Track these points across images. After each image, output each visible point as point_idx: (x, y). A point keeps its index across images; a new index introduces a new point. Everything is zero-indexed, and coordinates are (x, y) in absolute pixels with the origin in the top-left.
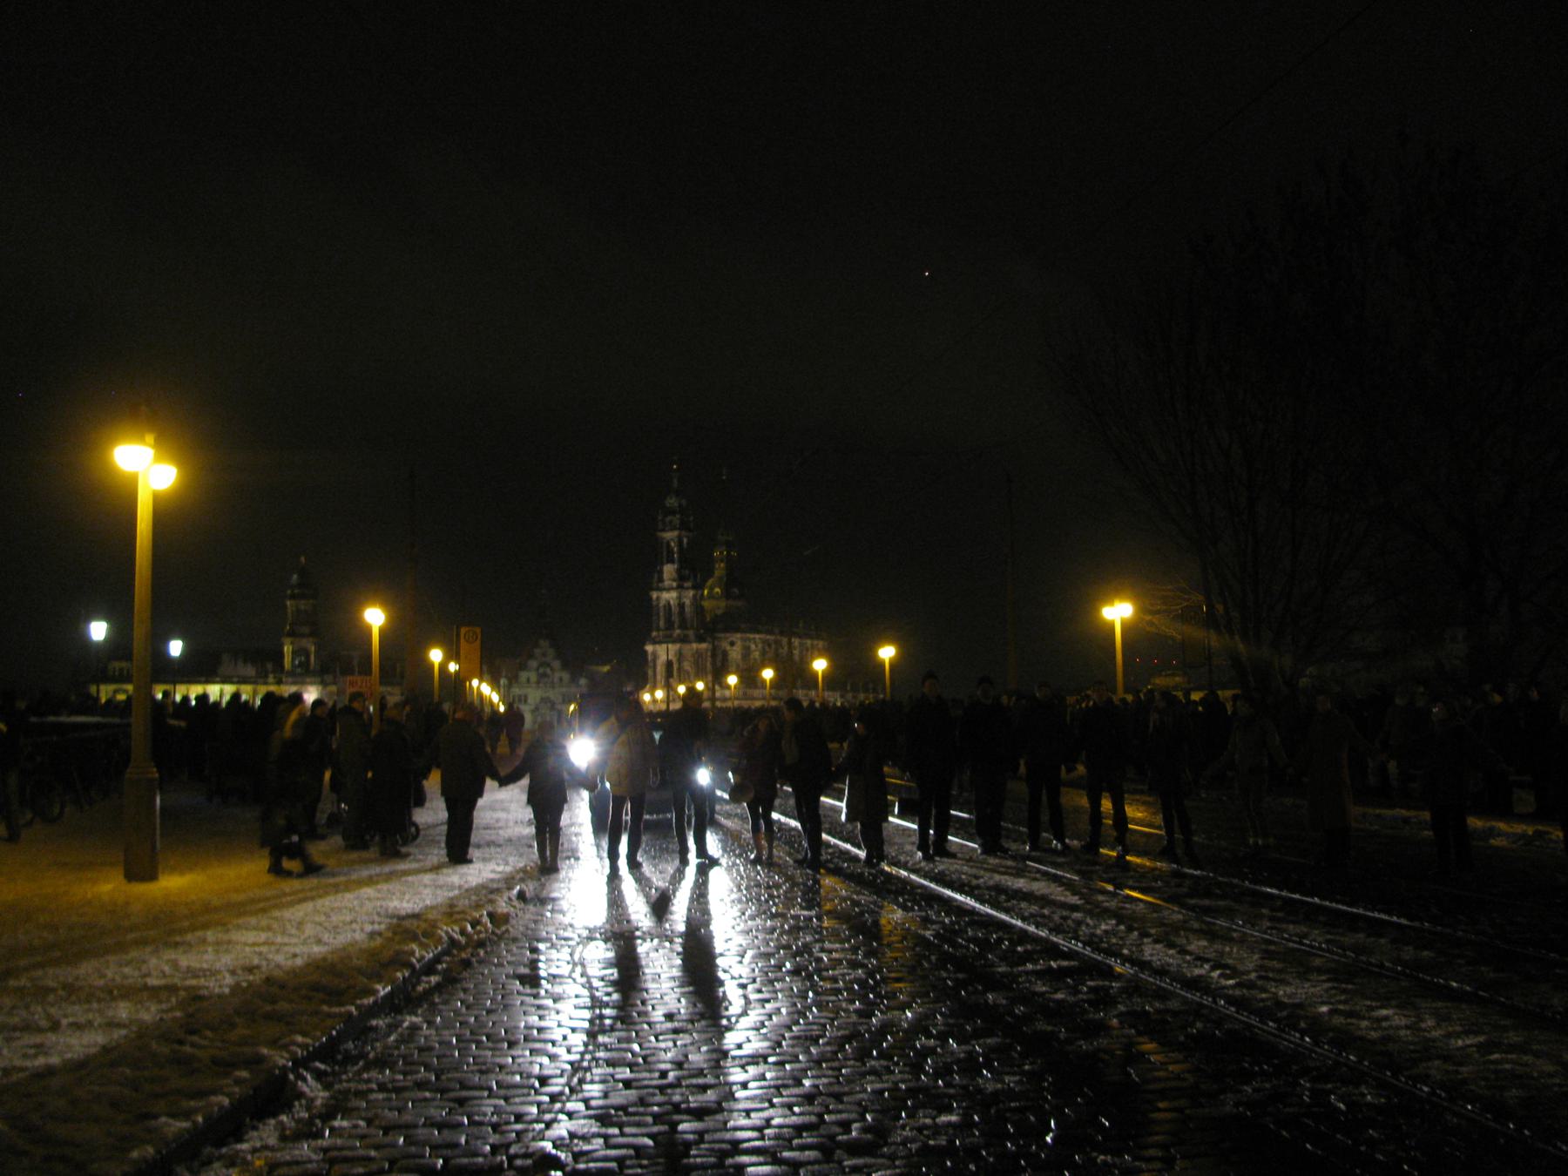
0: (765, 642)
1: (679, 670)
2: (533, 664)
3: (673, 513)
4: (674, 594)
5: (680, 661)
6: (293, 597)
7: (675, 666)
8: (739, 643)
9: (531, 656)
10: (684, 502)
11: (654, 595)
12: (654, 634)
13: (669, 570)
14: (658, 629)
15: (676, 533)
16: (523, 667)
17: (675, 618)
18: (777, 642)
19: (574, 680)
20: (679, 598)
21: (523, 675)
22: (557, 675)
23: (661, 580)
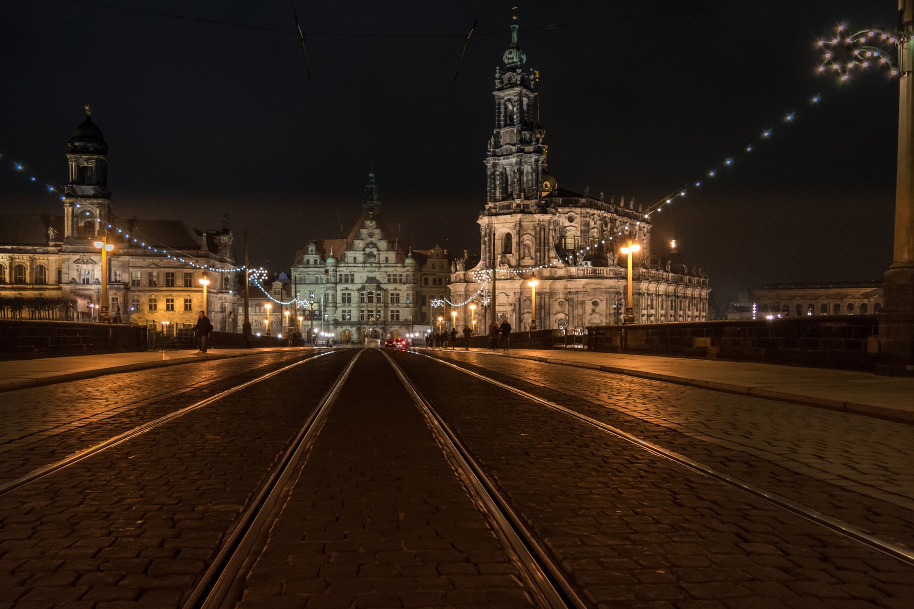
0: (603, 219)
1: (519, 243)
2: (359, 244)
3: (513, 69)
4: (513, 160)
5: (519, 234)
6: (74, 151)
7: (514, 240)
8: (578, 219)
9: (358, 237)
10: (524, 57)
13: (507, 135)
14: (495, 201)
15: (517, 89)
16: (350, 247)
18: (613, 221)
19: (401, 260)
20: (520, 163)
21: (350, 255)
22: (383, 256)
23: (498, 145)
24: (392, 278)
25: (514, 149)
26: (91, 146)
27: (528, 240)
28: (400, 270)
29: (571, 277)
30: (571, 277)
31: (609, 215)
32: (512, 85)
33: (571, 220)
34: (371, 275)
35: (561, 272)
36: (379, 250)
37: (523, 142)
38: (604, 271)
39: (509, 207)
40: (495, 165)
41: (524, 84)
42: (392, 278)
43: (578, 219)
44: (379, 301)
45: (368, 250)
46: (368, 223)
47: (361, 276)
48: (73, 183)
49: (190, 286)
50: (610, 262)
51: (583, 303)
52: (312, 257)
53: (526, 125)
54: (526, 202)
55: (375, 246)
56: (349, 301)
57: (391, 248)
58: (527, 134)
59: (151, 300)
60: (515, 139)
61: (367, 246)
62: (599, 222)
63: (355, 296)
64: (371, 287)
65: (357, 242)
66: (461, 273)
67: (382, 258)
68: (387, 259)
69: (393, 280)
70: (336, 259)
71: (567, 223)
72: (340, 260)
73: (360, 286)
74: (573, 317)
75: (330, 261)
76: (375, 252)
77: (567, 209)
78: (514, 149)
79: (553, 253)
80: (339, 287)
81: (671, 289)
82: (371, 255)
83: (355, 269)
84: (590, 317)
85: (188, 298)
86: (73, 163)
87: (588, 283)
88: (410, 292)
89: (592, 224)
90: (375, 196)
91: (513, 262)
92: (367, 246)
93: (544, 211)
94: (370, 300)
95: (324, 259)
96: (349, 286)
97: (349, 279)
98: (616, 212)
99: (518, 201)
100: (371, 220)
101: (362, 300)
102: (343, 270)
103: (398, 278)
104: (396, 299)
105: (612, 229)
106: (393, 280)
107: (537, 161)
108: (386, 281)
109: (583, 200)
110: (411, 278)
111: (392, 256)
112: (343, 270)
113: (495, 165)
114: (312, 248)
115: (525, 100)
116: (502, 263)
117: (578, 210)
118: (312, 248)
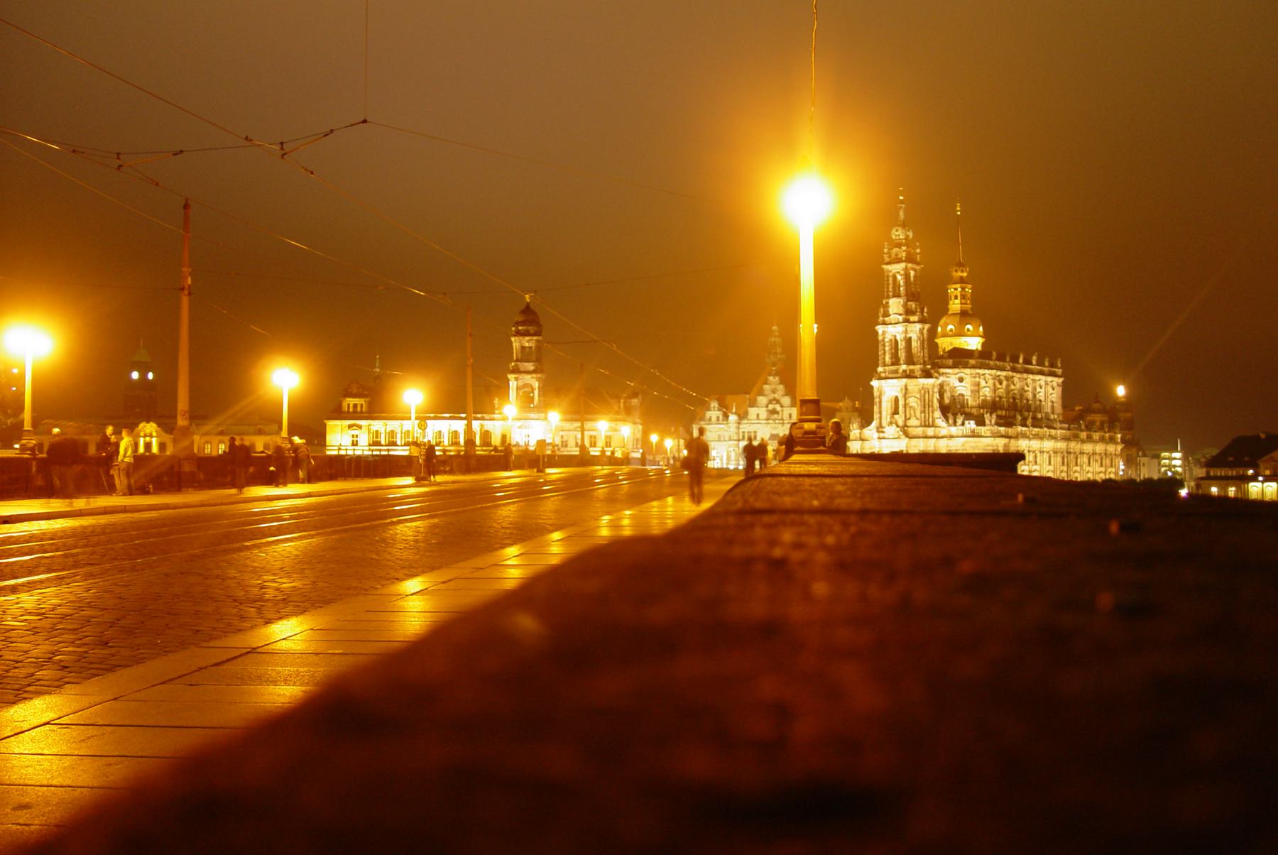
0: (996, 378)
1: (905, 406)
2: (762, 400)
3: (899, 245)
4: (900, 328)
5: (905, 396)
6: (518, 333)
7: (901, 403)
8: (968, 380)
9: (761, 393)
10: (911, 234)
11: (880, 329)
12: (880, 369)
13: (895, 305)
14: (885, 365)
15: (903, 265)
16: (753, 404)
17: (902, 355)
21: (753, 411)
22: (786, 412)
23: (887, 314)
25: (901, 318)
26: (532, 329)
27: (913, 402)
29: (951, 437)
30: (951, 437)
31: (1004, 373)
32: (899, 261)
33: (961, 380)
34: (775, 432)
35: (943, 432)
37: (908, 312)
38: (982, 430)
39: (896, 372)
40: (884, 333)
41: (910, 259)
43: (968, 380)
45: (771, 407)
46: (771, 378)
48: (517, 360)
50: (987, 422)
52: (714, 413)
53: (911, 296)
54: (912, 367)
55: (778, 402)
58: (912, 305)
60: (901, 310)
61: (770, 402)
62: (991, 382)
65: (766, 387)
66: (857, 432)
67: (786, 415)
71: (957, 383)
72: (742, 416)
75: (733, 418)
76: (778, 408)
77: (956, 370)
78: (901, 318)
79: (938, 414)
81: (1061, 445)
82: (774, 412)
86: (516, 342)
89: (983, 383)
91: (901, 423)
92: (770, 402)
93: (928, 375)
95: (726, 416)
98: (1014, 370)
99: (904, 367)
100: (776, 375)
105: (1008, 386)
107: (921, 331)
109: (972, 362)
113: (884, 333)
114: (714, 404)
115: (912, 273)
116: (891, 423)
117: (968, 371)
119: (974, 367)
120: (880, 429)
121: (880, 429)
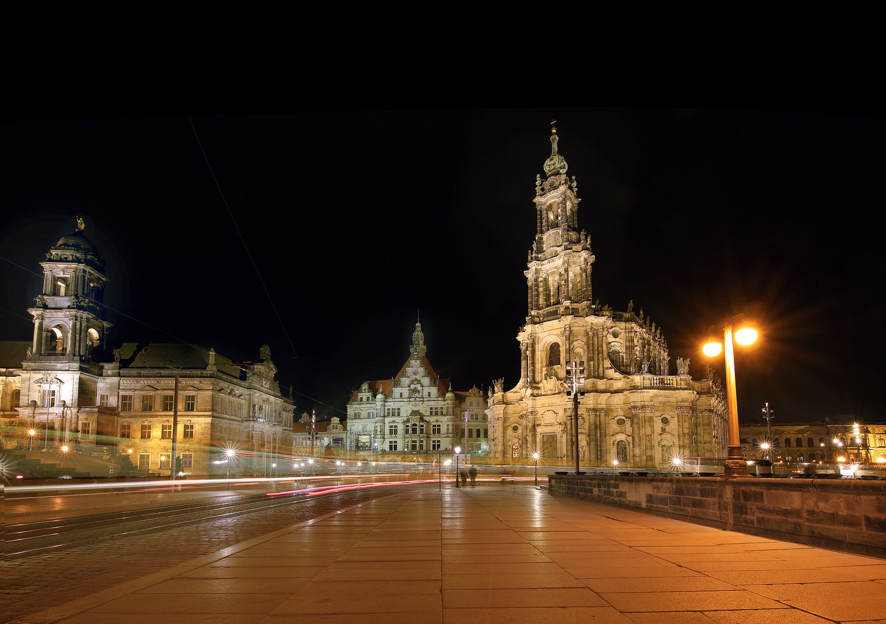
2: (405, 381)
16: (397, 385)
19: (442, 394)
21: (397, 391)
22: (426, 390)
24: (434, 410)
28: (441, 403)
29: (634, 388)
30: (634, 388)
34: (415, 409)
35: (618, 385)
36: (422, 386)
42: (434, 410)
44: (422, 431)
45: (413, 387)
46: (413, 362)
47: (406, 409)
49: (192, 410)
50: (680, 370)
51: (651, 419)
55: (419, 382)
56: (396, 432)
57: (433, 383)
59: (143, 427)
63: (401, 428)
64: (415, 420)
66: (499, 395)
67: (426, 394)
68: (429, 395)
69: (435, 412)
70: (385, 395)
72: (387, 396)
73: (405, 419)
74: (640, 438)
75: (380, 396)
76: (419, 388)
80: (387, 420)
82: (415, 391)
83: (402, 403)
84: (660, 438)
85: (188, 424)
87: (656, 396)
88: (451, 423)
90: (421, 342)
91: (562, 373)
92: (412, 382)
94: (414, 431)
95: (374, 396)
96: (396, 419)
97: (397, 413)
100: (416, 359)
101: (407, 431)
102: (390, 405)
103: (439, 410)
104: (436, 430)
106: (435, 412)
108: (429, 413)
110: (451, 411)
111: (434, 391)
112: (390, 405)
116: (548, 376)
118: (365, 386)
119: (627, 320)
120: (534, 384)
121: (534, 384)
